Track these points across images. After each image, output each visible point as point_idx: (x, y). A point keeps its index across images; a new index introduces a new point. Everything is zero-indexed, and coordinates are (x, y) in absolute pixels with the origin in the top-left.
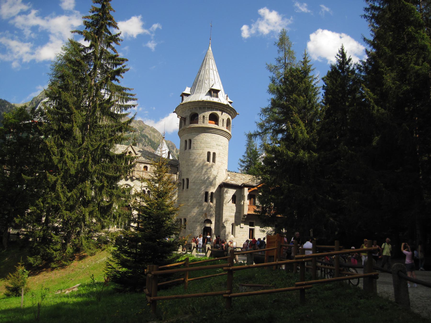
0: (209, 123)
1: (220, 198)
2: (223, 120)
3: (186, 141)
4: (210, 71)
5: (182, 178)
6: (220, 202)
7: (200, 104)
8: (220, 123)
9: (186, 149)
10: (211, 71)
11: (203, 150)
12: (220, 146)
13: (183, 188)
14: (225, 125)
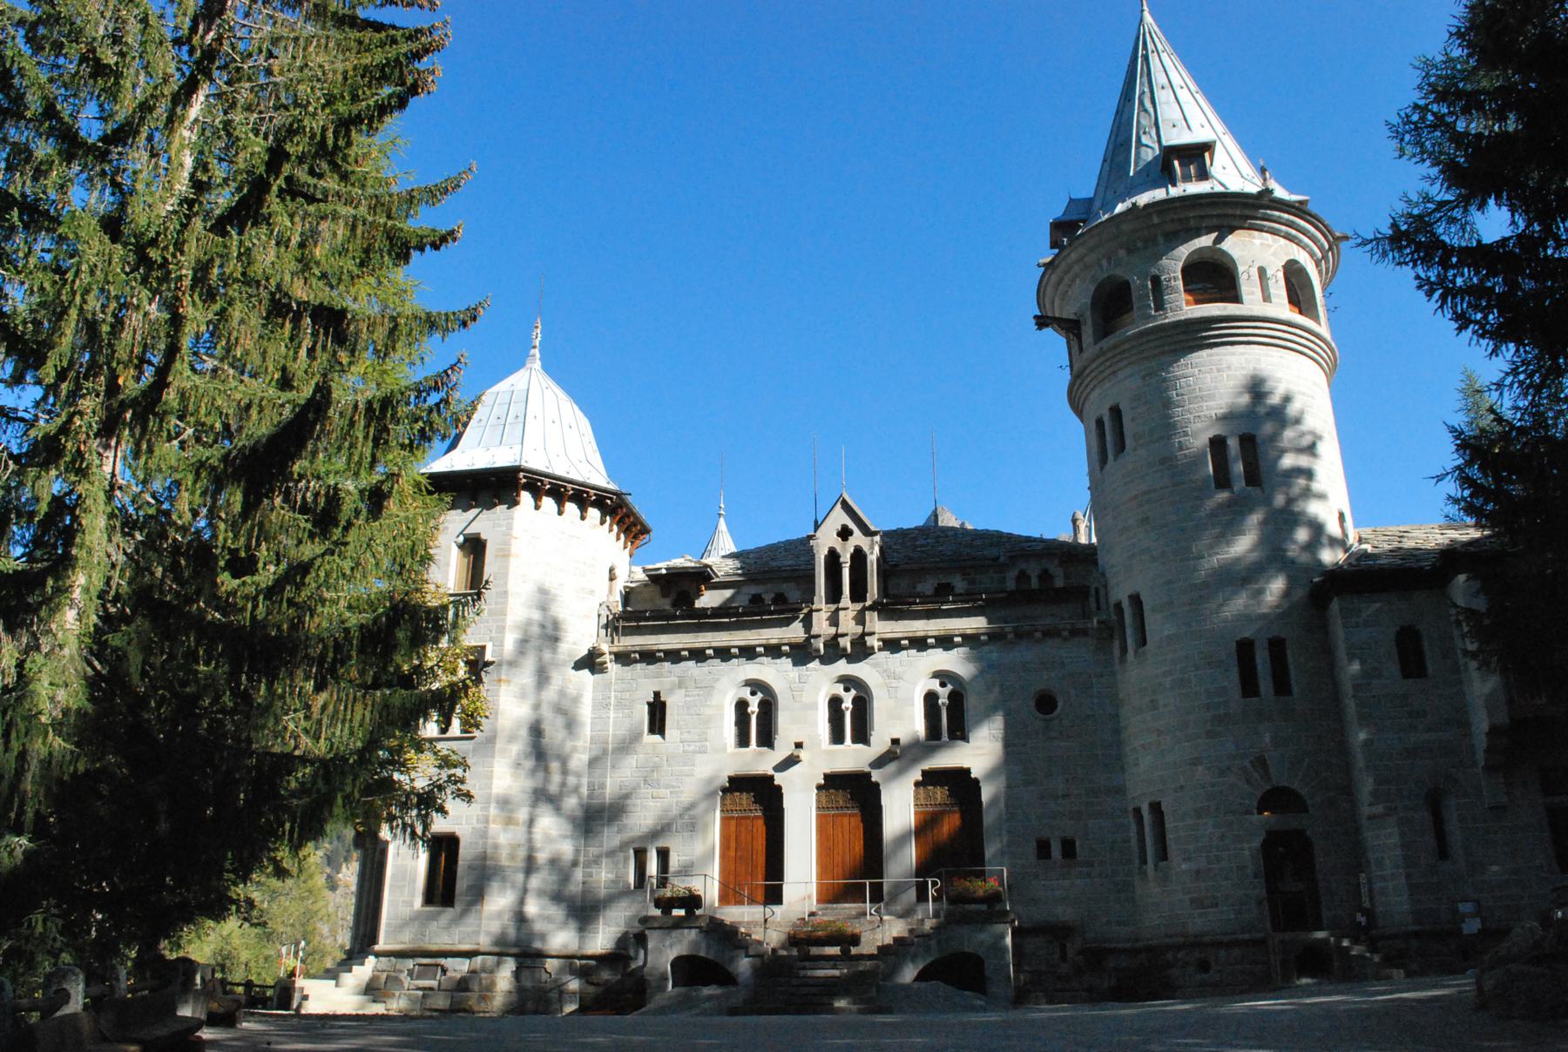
2: (1262, 272)
3: (1100, 423)
4: (1158, 94)
5: (1112, 601)
7: (1125, 227)
8: (1249, 287)
9: (1103, 460)
10: (1163, 96)
13: (1124, 650)
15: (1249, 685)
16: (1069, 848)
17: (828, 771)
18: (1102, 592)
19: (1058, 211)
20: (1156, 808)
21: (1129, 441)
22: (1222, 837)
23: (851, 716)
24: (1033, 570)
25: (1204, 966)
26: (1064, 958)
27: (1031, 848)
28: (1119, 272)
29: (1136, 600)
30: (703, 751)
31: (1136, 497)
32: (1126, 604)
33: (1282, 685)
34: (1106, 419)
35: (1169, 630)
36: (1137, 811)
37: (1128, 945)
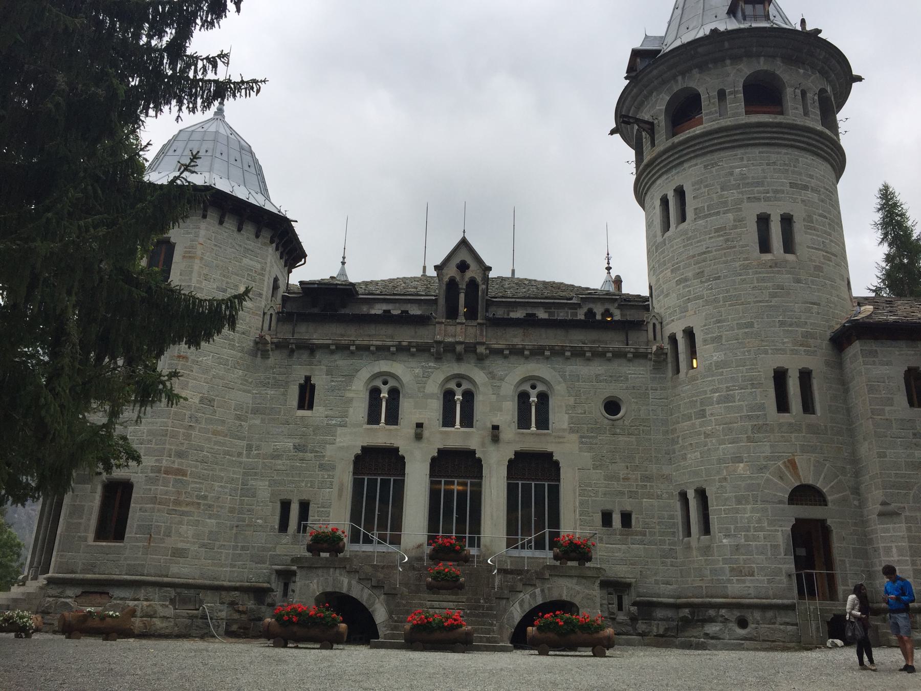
0: (747, 113)
1: (847, 391)
5: (667, 334)
6: (849, 411)
9: (666, 226)
11: (740, 210)
12: (805, 188)
13: (678, 371)
14: (815, 111)
15: (783, 405)
16: (626, 519)
17: (441, 447)
18: (658, 327)
20: (702, 494)
21: (690, 214)
22: (759, 521)
23: (458, 406)
24: (599, 310)
25: (743, 623)
26: (620, 608)
27: (598, 518)
29: (690, 334)
30: (344, 425)
31: (694, 256)
32: (680, 337)
33: (808, 406)
35: (717, 357)
36: (683, 496)
37: (671, 600)
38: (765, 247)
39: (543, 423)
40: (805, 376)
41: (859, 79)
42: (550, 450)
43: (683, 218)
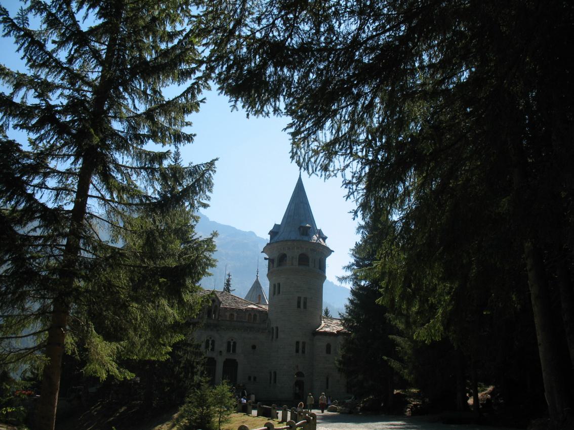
3: (275, 285)
9: (274, 294)
16: (255, 378)
19: (271, 228)
20: (275, 373)
21: (281, 292)
28: (285, 252)
29: (277, 328)
33: (303, 352)
34: (276, 284)
36: (271, 373)
38: (299, 306)
39: (234, 351)
40: (304, 343)
41: (333, 251)
42: (235, 358)
43: (279, 293)
